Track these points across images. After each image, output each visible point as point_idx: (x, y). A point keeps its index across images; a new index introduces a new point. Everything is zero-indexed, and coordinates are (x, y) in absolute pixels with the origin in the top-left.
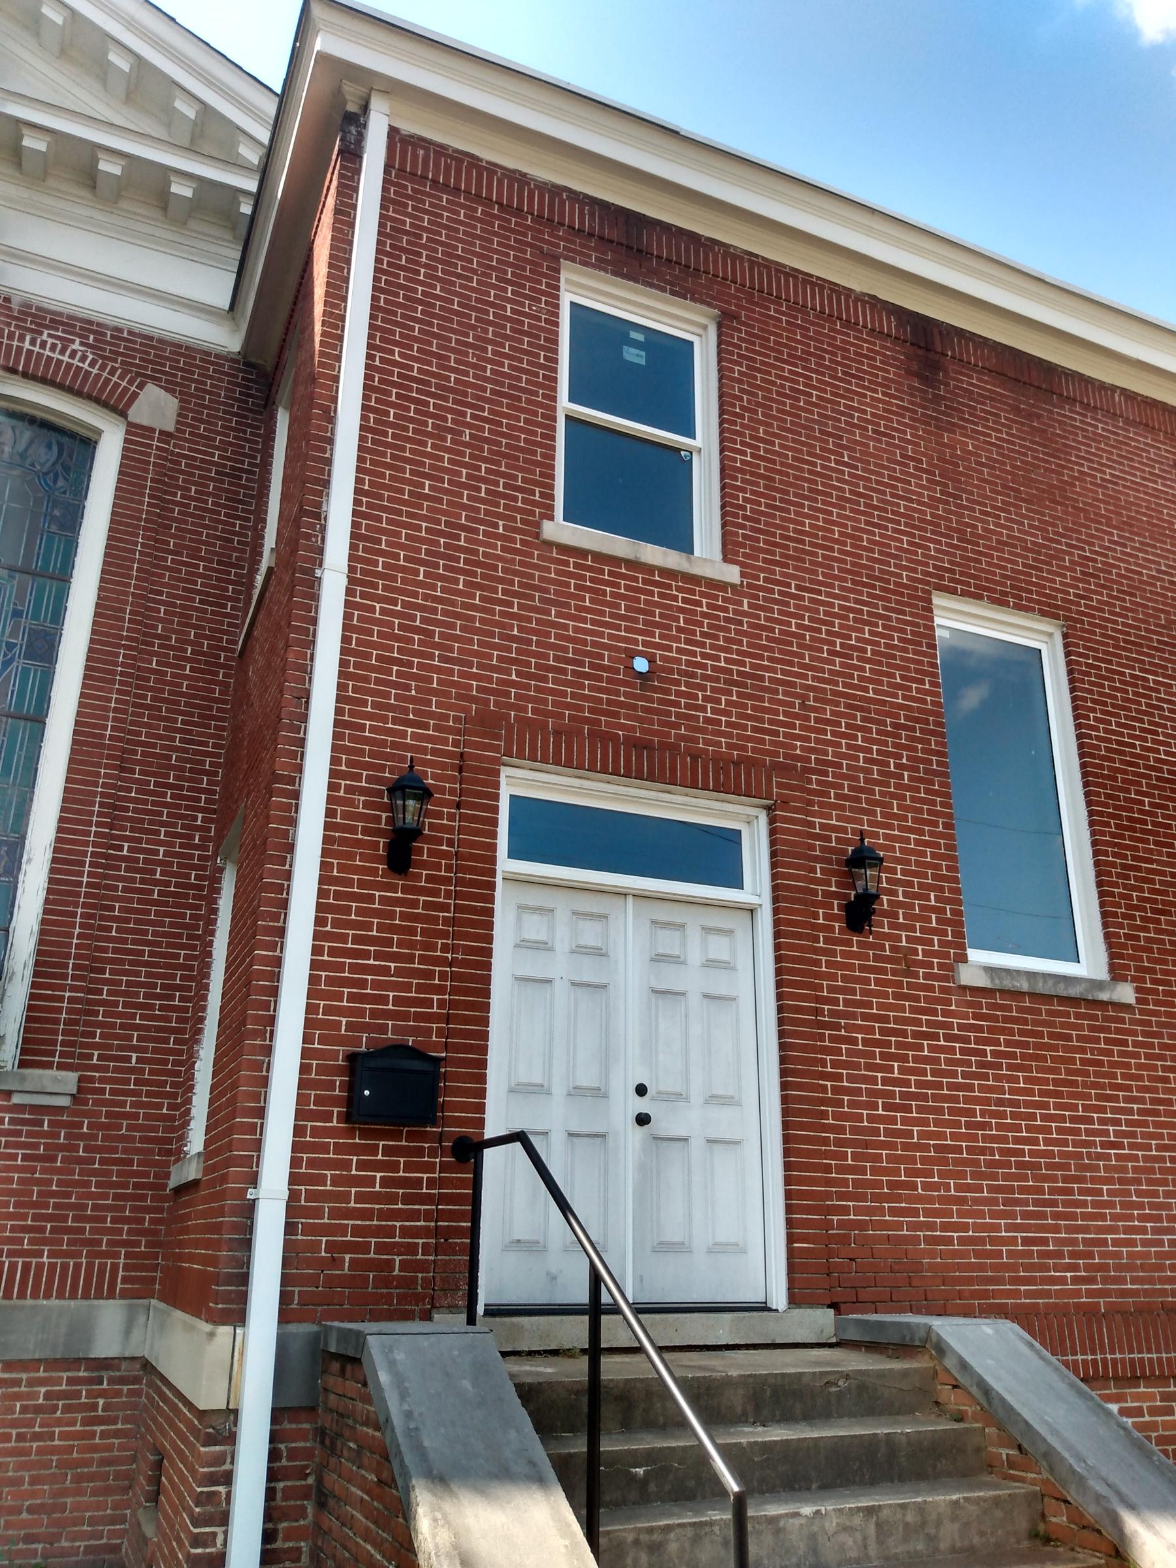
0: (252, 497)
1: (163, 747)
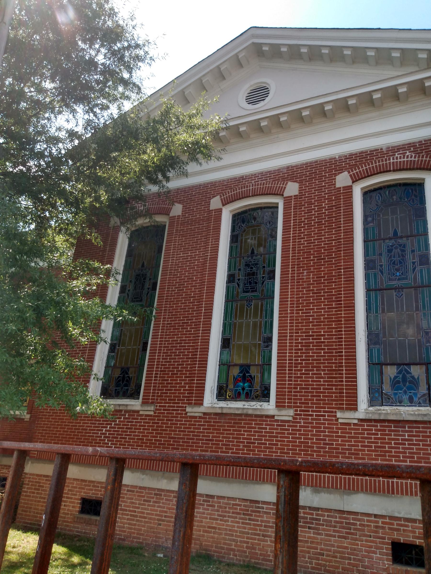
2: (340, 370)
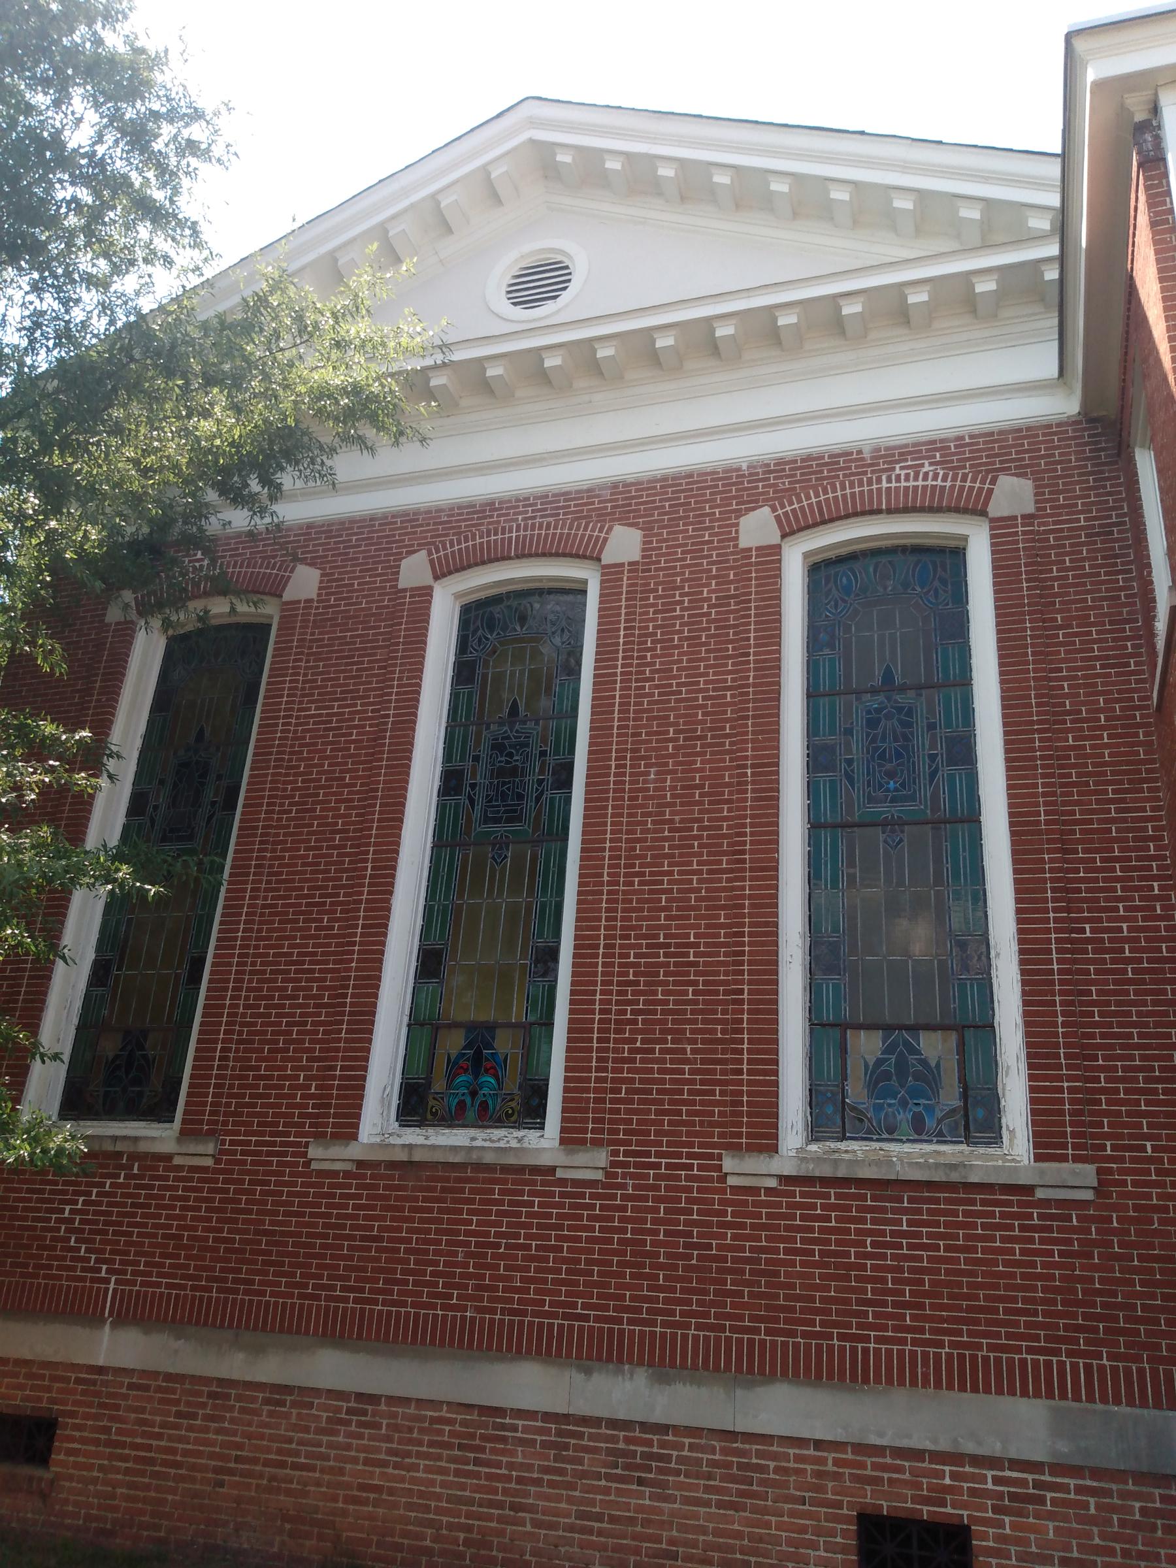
0: (1129, 547)
1: (1100, 821)
2: (734, 1041)
